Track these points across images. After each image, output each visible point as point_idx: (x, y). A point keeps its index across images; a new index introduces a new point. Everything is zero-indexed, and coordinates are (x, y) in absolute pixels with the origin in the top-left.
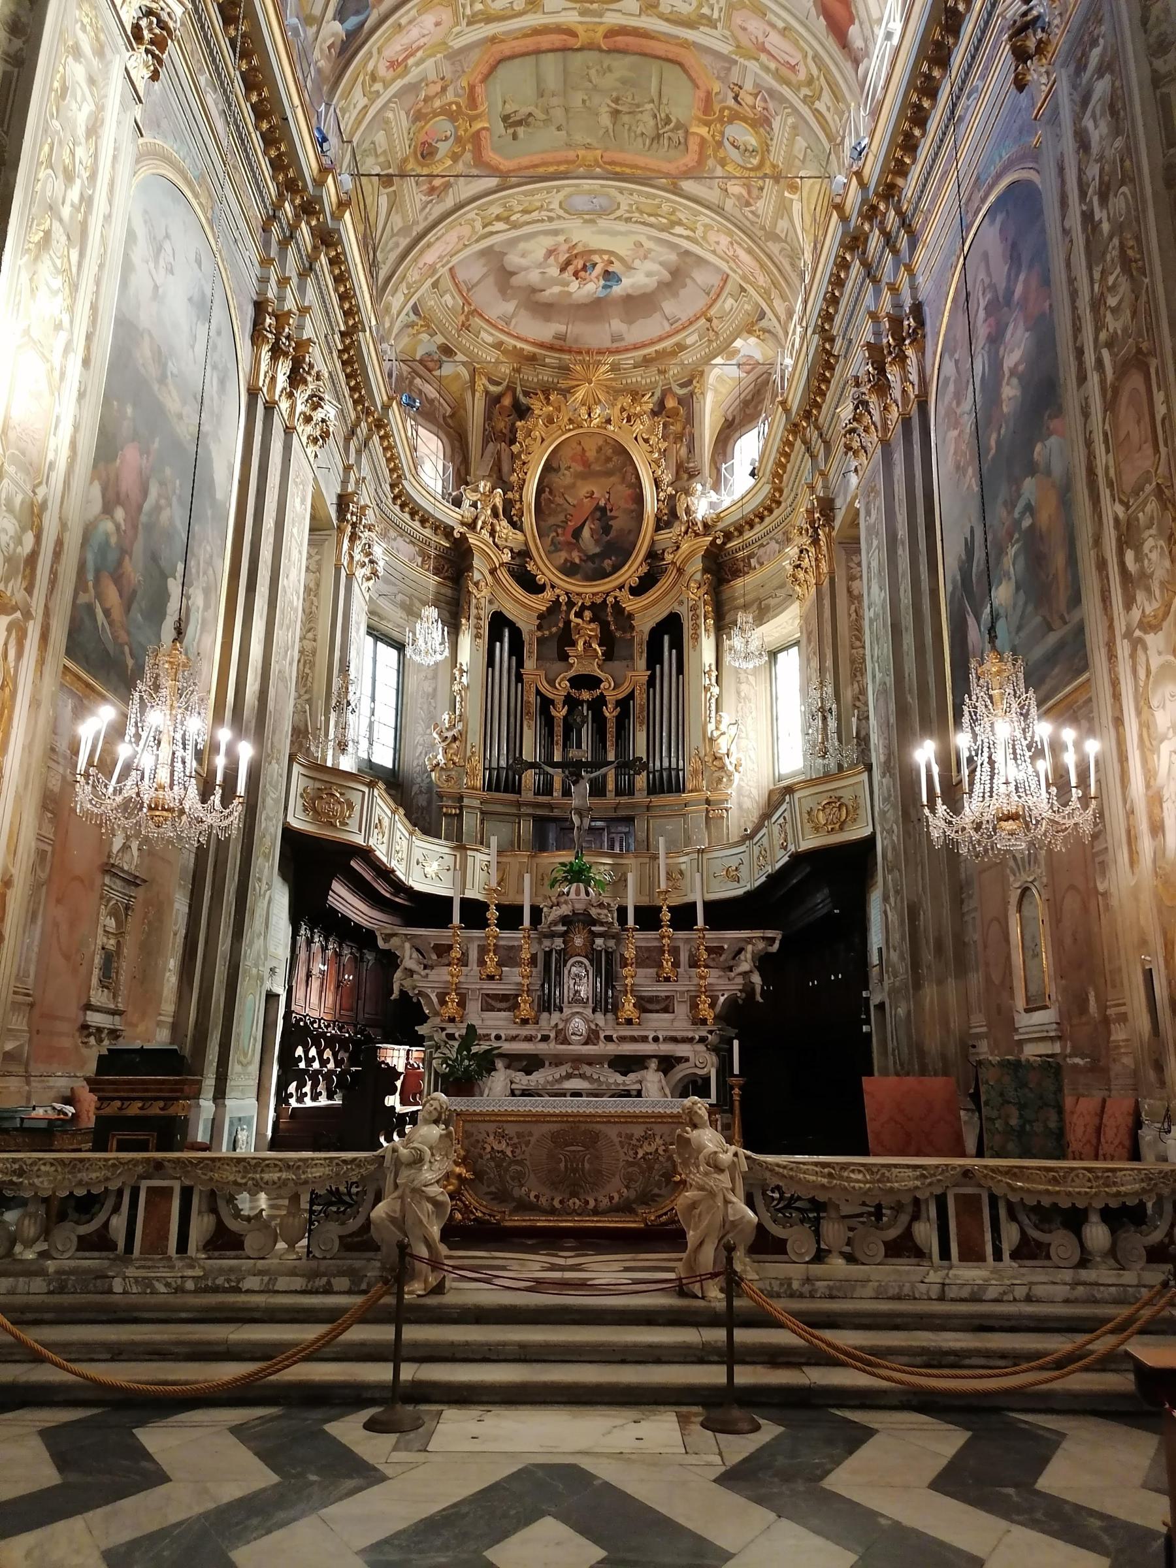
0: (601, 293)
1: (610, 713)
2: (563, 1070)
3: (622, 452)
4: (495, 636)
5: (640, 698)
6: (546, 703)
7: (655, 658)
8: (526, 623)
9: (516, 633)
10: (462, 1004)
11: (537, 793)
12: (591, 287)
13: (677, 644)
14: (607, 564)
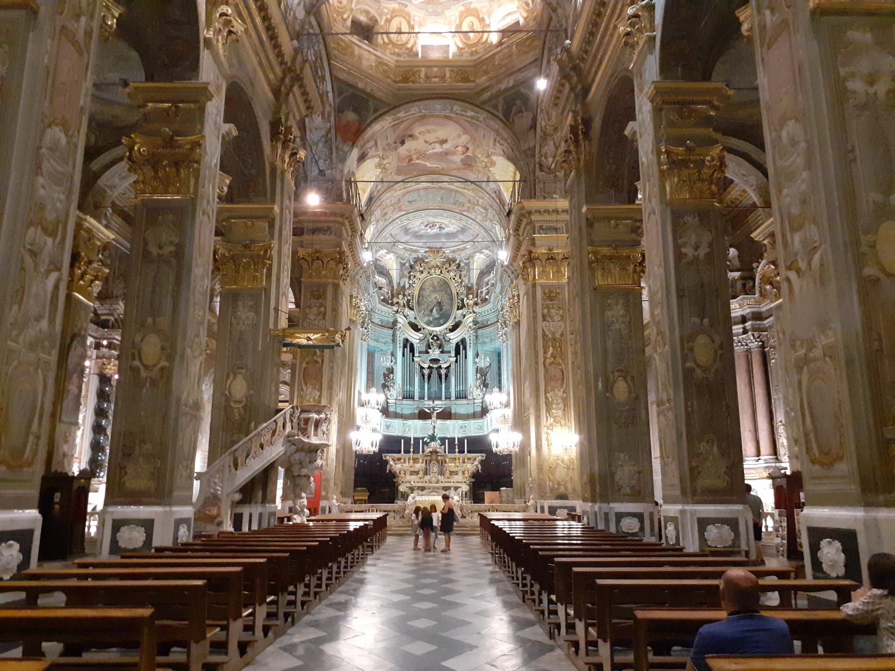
0: (438, 232)
1: (443, 372)
2: (431, 490)
3: (446, 283)
4: (405, 346)
5: (453, 367)
6: (422, 368)
7: (457, 353)
8: (415, 342)
9: (412, 346)
10: (405, 474)
11: (420, 398)
12: (435, 230)
13: (465, 348)
14: (442, 321)
